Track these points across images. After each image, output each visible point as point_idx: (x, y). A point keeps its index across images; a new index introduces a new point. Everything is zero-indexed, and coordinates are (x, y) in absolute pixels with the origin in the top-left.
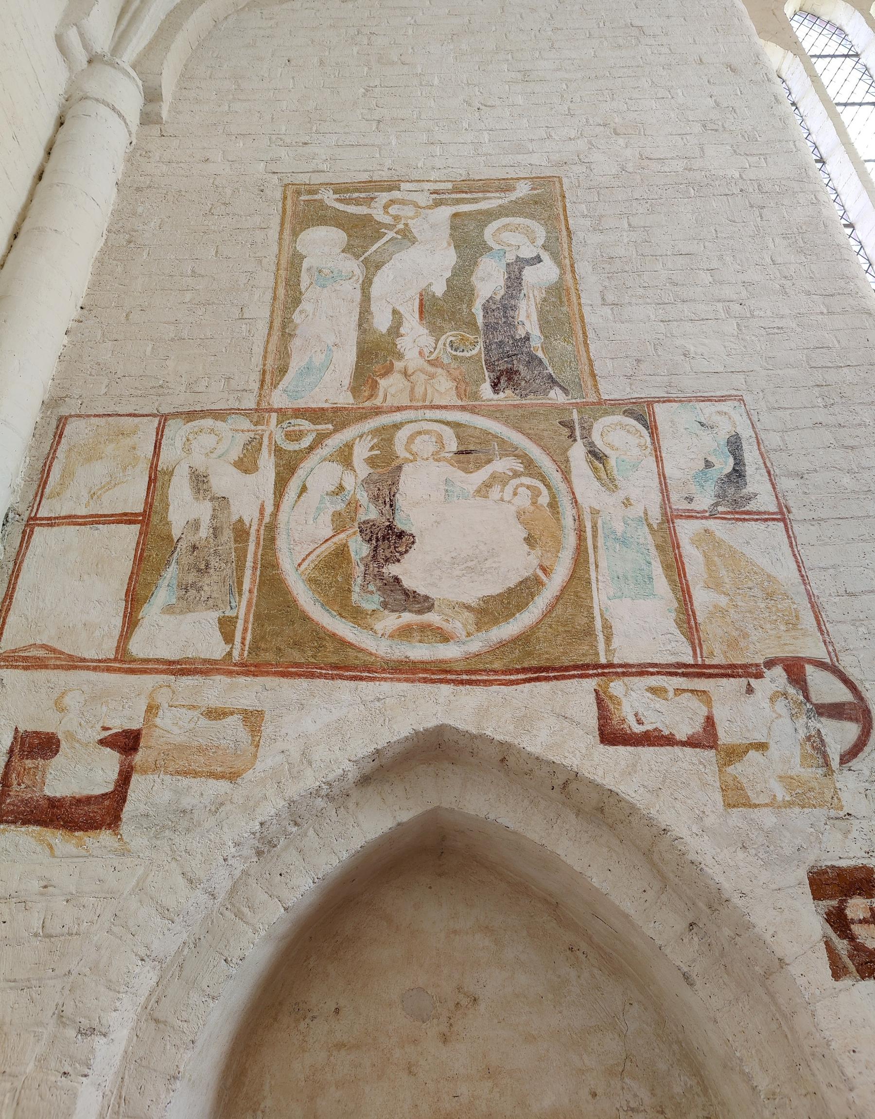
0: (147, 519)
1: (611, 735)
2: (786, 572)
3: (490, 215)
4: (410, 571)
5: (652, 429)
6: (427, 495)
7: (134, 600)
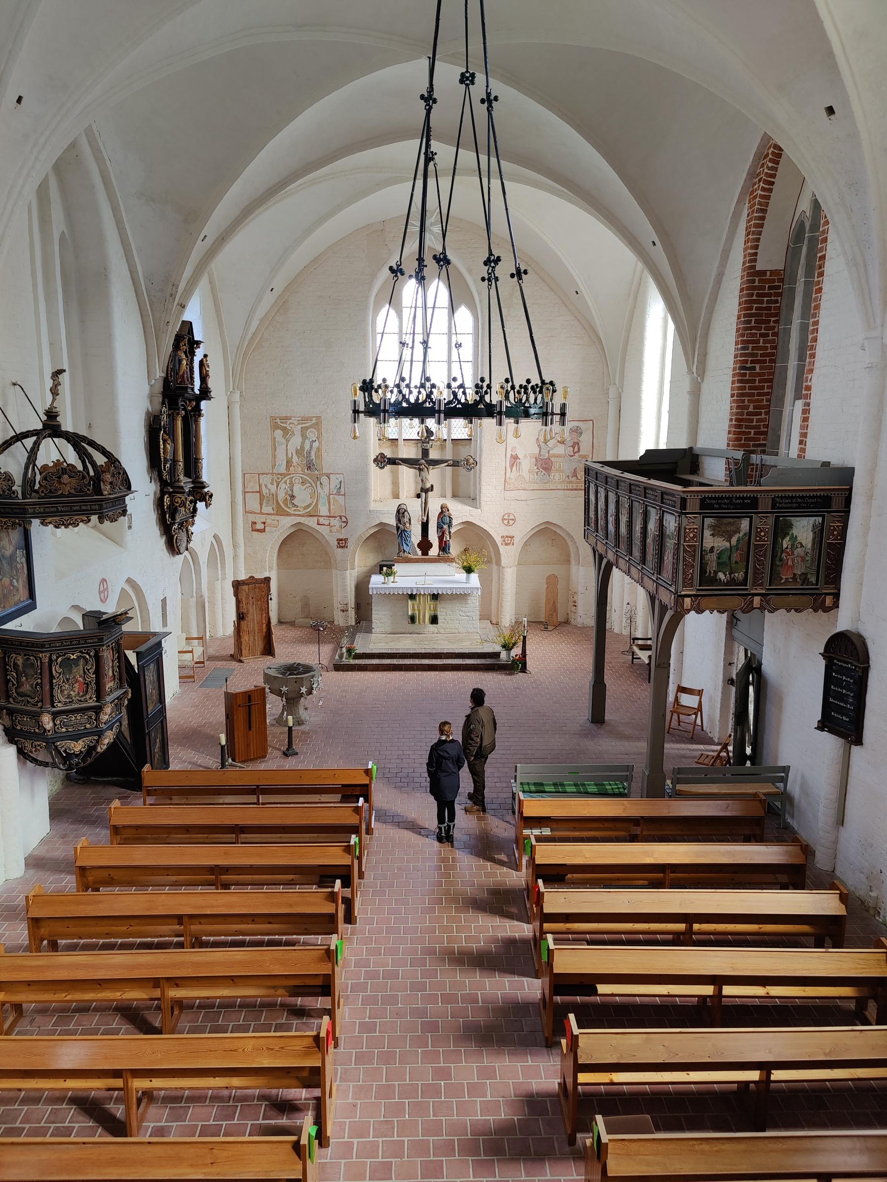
0: (260, 492)
3: (307, 428)
4: (295, 502)
6: (297, 488)
7: (261, 505)
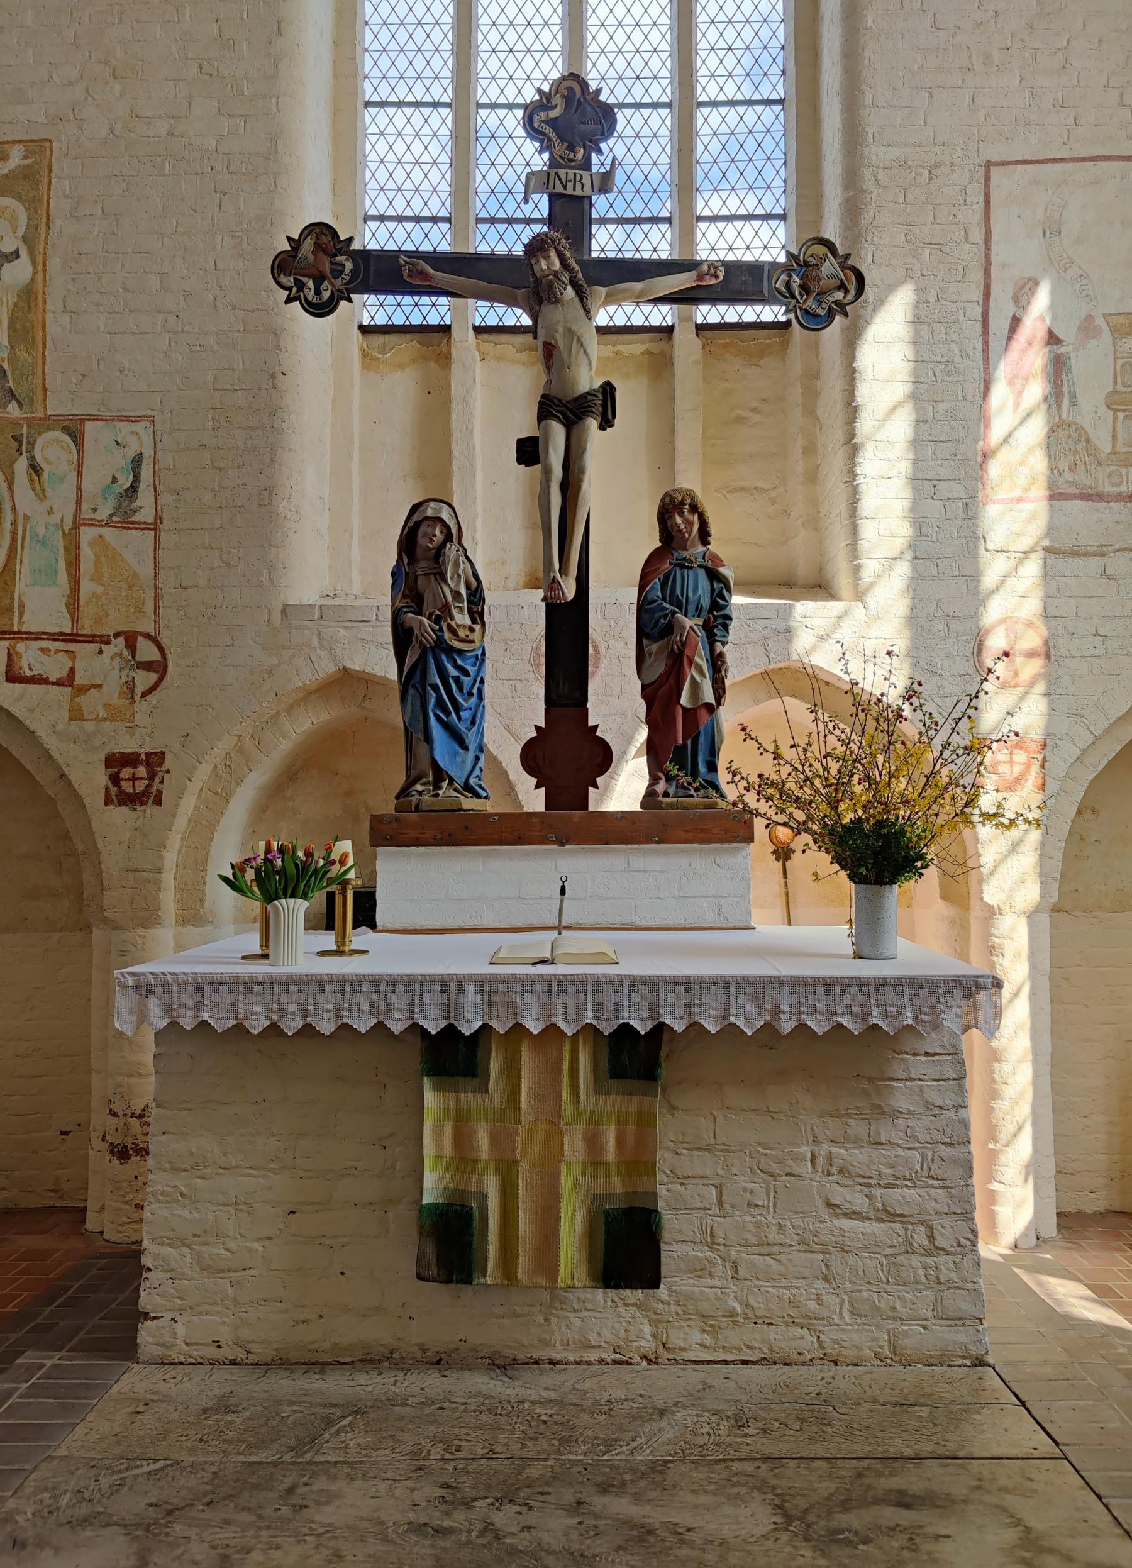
1: (12, 677)
2: (146, 571)
5: (79, 443)
